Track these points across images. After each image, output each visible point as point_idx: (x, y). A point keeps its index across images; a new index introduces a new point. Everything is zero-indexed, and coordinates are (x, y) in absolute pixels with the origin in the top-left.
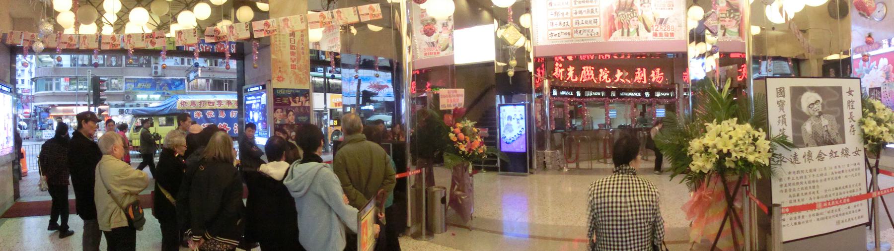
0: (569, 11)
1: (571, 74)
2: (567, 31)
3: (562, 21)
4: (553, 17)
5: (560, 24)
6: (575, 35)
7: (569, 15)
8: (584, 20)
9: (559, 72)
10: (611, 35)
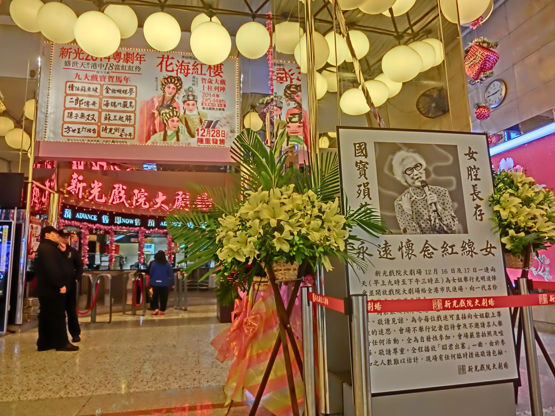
0: (97, 100)
1: (95, 192)
2: (92, 127)
3: (86, 113)
4: (73, 105)
5: (83, 116)
6: (103, 134)
7: (97, 105)
8: (118, 115)
9: (76, 186)
10: (148, 138)
